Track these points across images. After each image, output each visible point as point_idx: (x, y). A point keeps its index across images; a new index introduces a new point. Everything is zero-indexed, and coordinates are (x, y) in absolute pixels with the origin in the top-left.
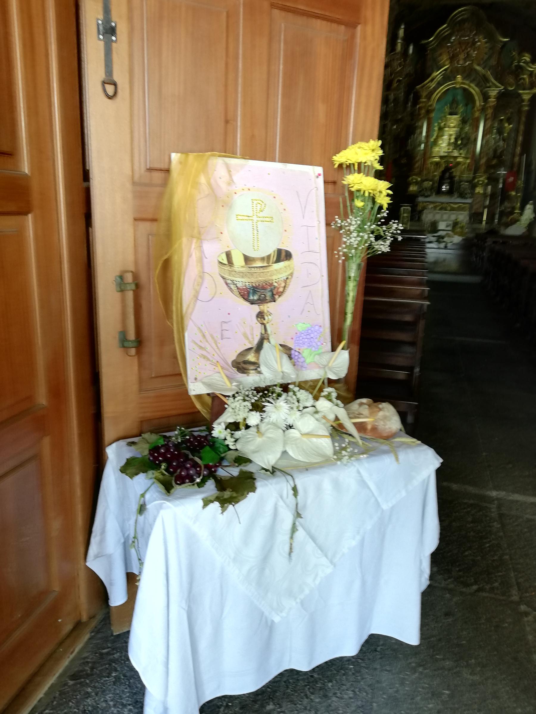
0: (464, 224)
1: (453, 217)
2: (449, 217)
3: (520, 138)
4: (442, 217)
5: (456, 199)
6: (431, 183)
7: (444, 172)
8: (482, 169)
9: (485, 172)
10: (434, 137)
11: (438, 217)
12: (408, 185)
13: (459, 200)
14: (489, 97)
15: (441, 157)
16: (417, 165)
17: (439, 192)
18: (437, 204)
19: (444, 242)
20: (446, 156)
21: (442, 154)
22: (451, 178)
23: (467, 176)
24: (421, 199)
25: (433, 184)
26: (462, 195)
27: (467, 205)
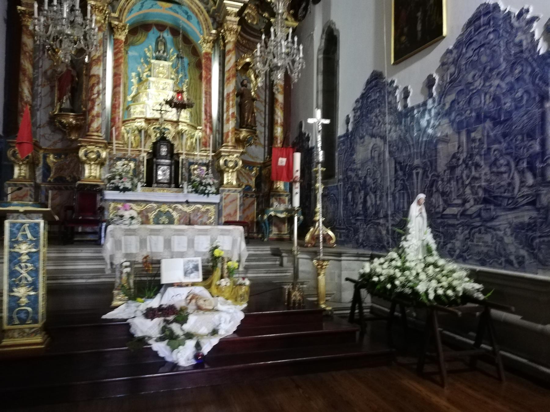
0: (233, 264)
1: (203, 244)
2: (191, 243)
3: (280, 98)
4: (168, 243)
5: (186, 194)
6: (132, 165)
7: (156, 147)
8: (231, 139)
9: (234, 147)
10: (133, 94)
11: (156, 246)
12: (80, 164)
13: (194, 197)
14: (227, 14)
15: (148, 121)
16: (95, 125)
17: (151, 181)
18: (149, 206)
19: (189, 336)
20: (157, 120)
21: (149, 116)
22: (172, 155)
23: (203, 155)
24: (110, 195)
25: (137, 166)
26: (199, 188)
27: (211, 208)
